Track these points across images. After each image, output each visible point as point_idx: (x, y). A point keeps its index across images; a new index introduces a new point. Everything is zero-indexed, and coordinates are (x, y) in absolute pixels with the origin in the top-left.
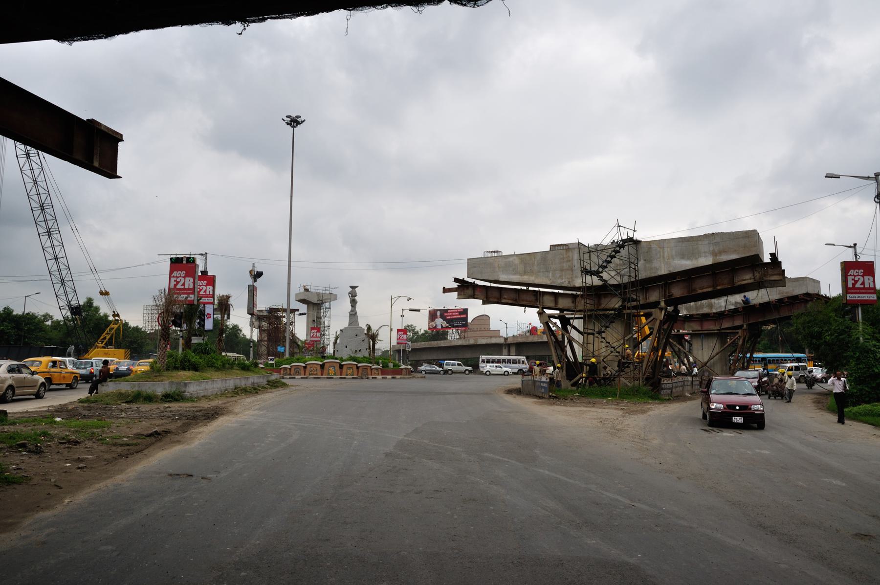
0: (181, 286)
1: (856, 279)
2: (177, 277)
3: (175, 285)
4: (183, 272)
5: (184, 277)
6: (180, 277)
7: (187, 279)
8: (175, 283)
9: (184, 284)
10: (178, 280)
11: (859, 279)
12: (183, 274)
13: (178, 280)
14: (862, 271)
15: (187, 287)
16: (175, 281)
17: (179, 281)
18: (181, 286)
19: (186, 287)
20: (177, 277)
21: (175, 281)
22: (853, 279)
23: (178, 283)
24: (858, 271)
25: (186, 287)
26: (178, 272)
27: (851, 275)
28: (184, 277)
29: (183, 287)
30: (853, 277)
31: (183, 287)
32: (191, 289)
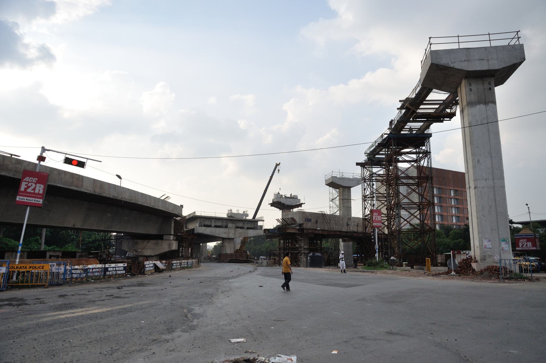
0: (32, 190)
1: (523, 243)
2: (29, 182)
3: (26, 189)
4: (35, 179)
5: (36, 183)
6: (32, 182)
7: (38, 185)
8: (26, 187)
9: (34, 189)
10: (30, 185)
11: (525, 243)
12: (35, 180)
13: (30, 185)
14: (526, 240)
15: (37, 191)
16: (26, 185)
17: (30, 185)
18: (32, 190)
19: (36, 192)
20: (29, 182)
21: (26, 185)
22: (522, 244)
23: (28, 187)
24: (524, 240)
25: (36, 192)
26: (31, 178)
27: (521, 242)
28: (36, 183)
29: (33, 191)
30: (522, 243)
31: (33, 191)
32: (41, 194)
